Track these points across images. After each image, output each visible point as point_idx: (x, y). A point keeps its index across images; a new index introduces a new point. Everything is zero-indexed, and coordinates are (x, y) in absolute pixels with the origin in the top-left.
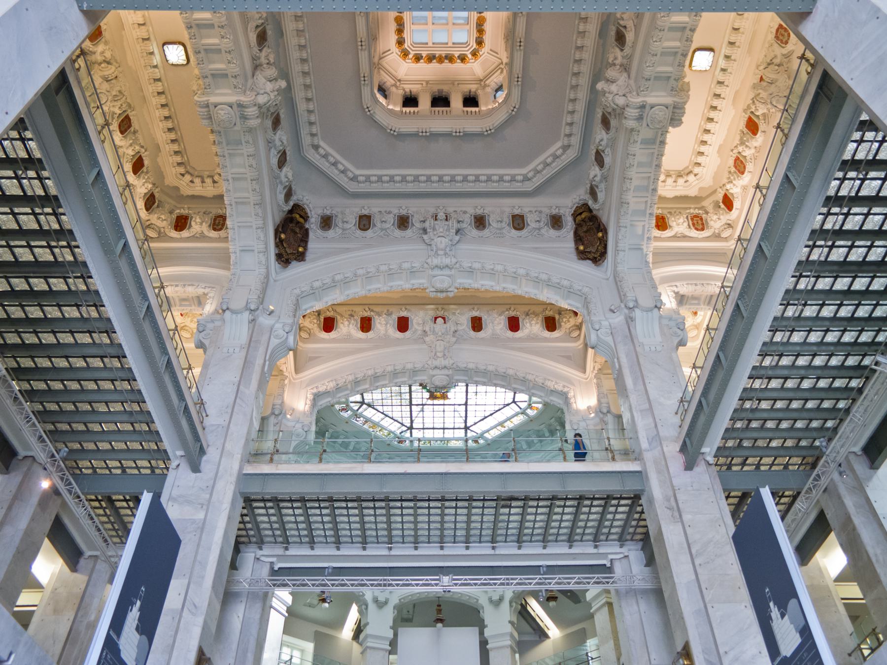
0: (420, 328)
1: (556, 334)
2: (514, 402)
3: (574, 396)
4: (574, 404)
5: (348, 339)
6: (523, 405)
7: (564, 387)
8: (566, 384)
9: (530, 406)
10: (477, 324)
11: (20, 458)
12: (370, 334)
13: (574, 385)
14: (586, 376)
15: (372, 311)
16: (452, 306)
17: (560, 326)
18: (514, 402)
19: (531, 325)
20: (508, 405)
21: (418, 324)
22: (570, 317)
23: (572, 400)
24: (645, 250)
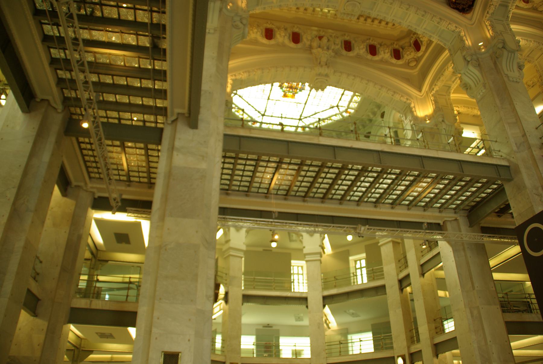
0: (308, 43)
1: (400, 62)
2: (337, 106)
3: (414, 107)
4: (415, 113)
5: (255, 42)
6: (342, 109)
7: (407, 99)
8: (408, 97)
9: (346, 111)
10: (348, 46)
11: (38, 100)
12: (272, 42)
13: (412, 98)
14: (421, 94)
15: (273, 24)
16: (330, 31)
17: (403, 57)
18: (337, 106)
19: (384, 53)
20: (333, 107)
21: (307, 40)
22: (412, 52)
23: (413, 109)
24: (510, 7)
